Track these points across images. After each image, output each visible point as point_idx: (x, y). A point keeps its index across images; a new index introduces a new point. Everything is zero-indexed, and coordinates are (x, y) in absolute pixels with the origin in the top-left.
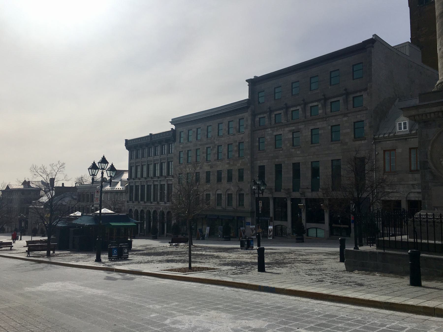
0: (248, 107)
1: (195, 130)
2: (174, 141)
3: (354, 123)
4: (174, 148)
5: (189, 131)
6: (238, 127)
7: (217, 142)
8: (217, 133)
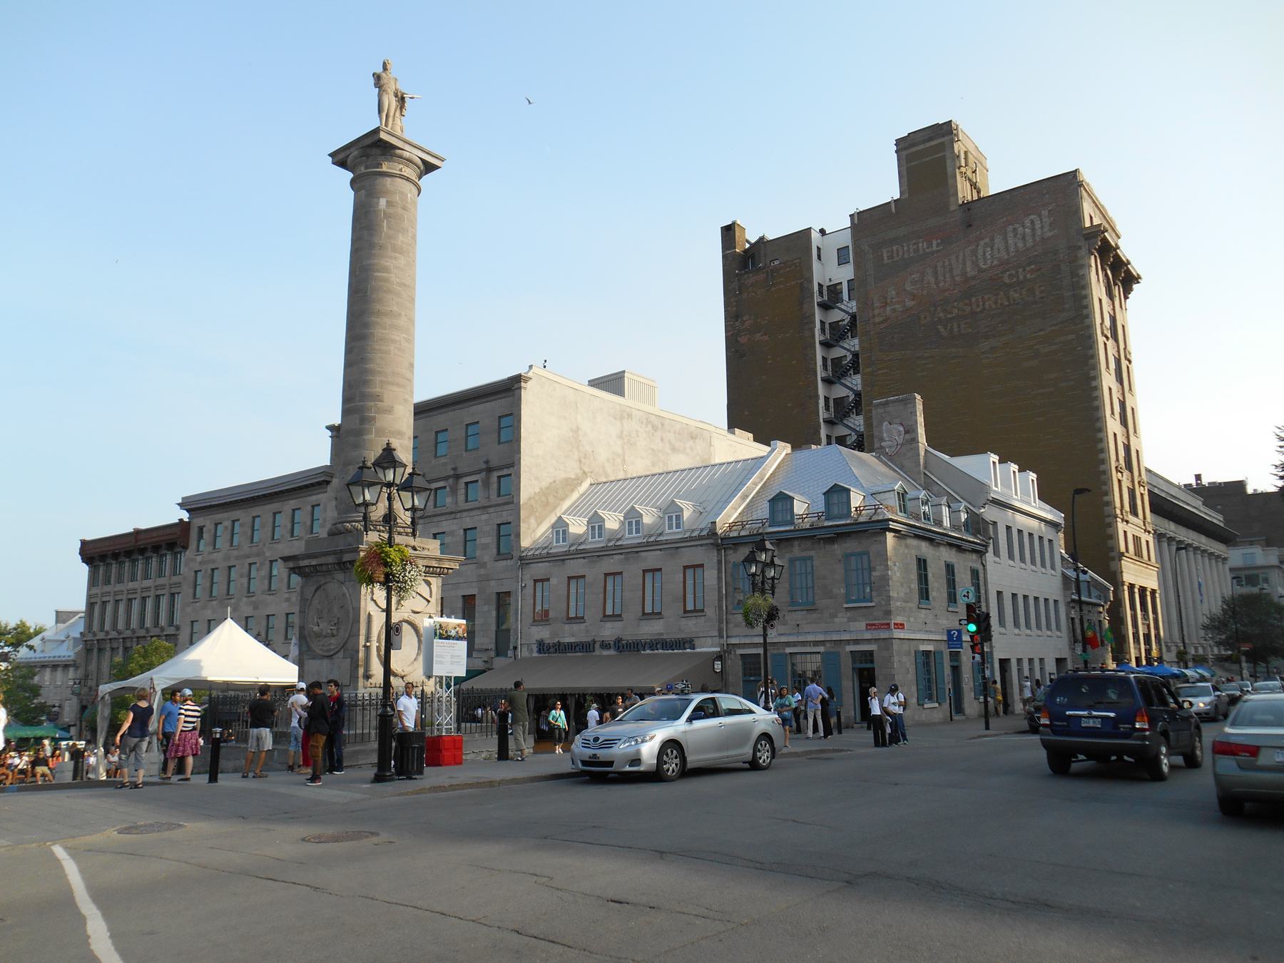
0: (328, 483)
1: (228, 523)
3: (499, 525)
4: (189, 560)
5: (216, 525)
6: (309, 523)
8: (270, 534)
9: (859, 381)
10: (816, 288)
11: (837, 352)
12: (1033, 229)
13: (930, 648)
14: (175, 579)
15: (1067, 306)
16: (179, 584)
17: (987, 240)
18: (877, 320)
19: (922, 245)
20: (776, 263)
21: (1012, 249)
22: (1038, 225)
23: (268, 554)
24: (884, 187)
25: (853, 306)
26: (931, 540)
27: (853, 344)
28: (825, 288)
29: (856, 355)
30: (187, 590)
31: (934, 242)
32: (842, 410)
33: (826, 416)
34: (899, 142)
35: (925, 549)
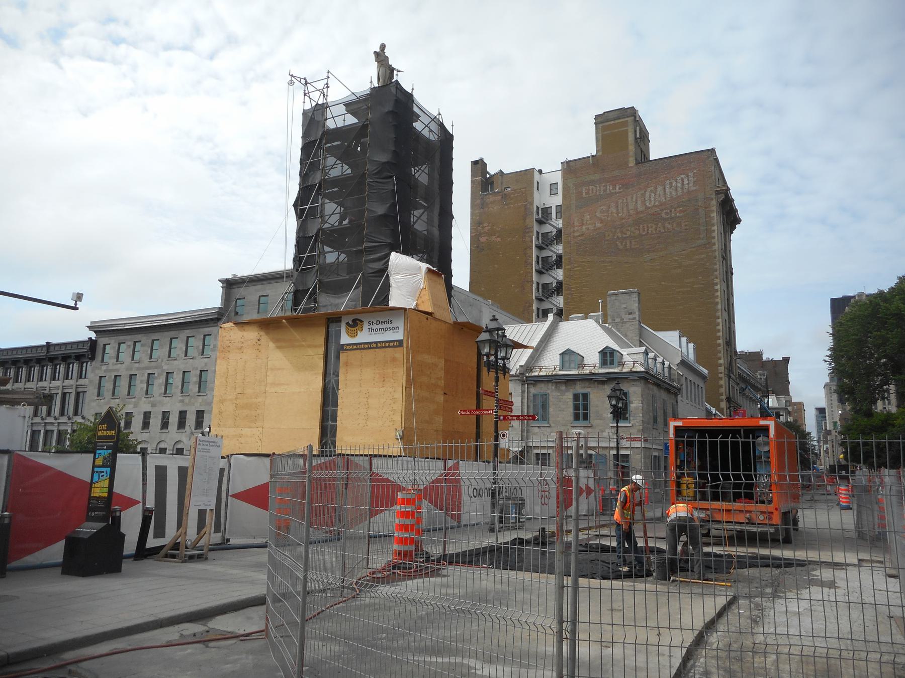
1: (131, 343)
2: (93, 358)
4: (93, 371)
7: (165, 367)
8: (167, 353)
9: (561, 274)
11: (546, 253)
12: (683, 184)
13: (656, 454)
14: (81, 382)
15: (701, 236)
16: (85, 386)
17: (652, 188)
18: (576, 234)
19: (610, 188)
21: (668, 195)
22: (686, 182)
23: (165, 367)
24: (586, 145)
25: (560, 223)
27: (559, 249)
30: (91, 392)
31: (618, 187)
32: (547, 292)
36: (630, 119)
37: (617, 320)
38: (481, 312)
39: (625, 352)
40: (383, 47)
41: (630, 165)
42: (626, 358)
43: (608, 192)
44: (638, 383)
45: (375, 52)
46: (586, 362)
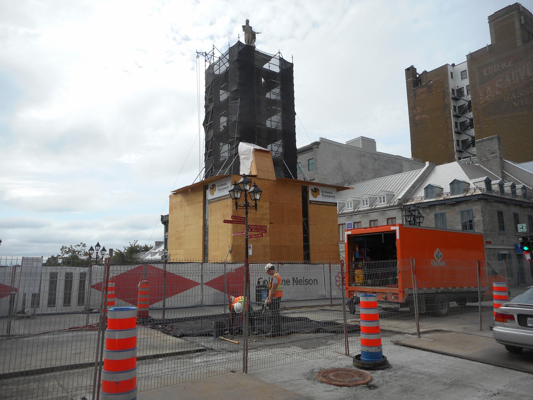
10: (451, 91)
11: (462, 120)
13: (506, 252)
18: (482, 102)
20: (431, 82)
25: (469, 98)
26: (505, 203)
27: (470, 115)
28: (455, 91)
29: (471, 120)
31: (510, 62)
33: (458, 148)
34: (490, 17)
35: (502, 207)
36: (515, 12)
37: (484, 159)
38: (402, 166)
39: (471, 182)
40: (247, 22)
41: (519, 45)
42: (472, 186)
43: (503, 68)
44: (478, 203)
45: (243, 26)
46: (444, 192)
